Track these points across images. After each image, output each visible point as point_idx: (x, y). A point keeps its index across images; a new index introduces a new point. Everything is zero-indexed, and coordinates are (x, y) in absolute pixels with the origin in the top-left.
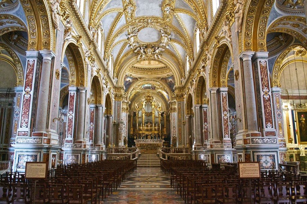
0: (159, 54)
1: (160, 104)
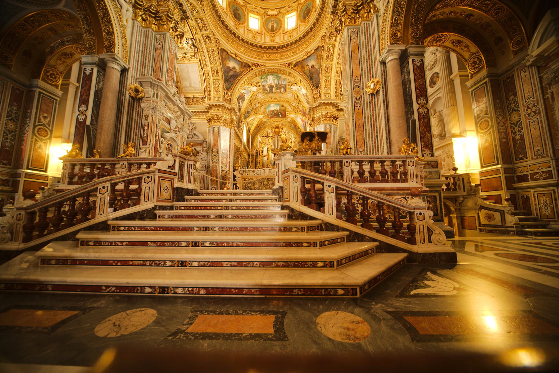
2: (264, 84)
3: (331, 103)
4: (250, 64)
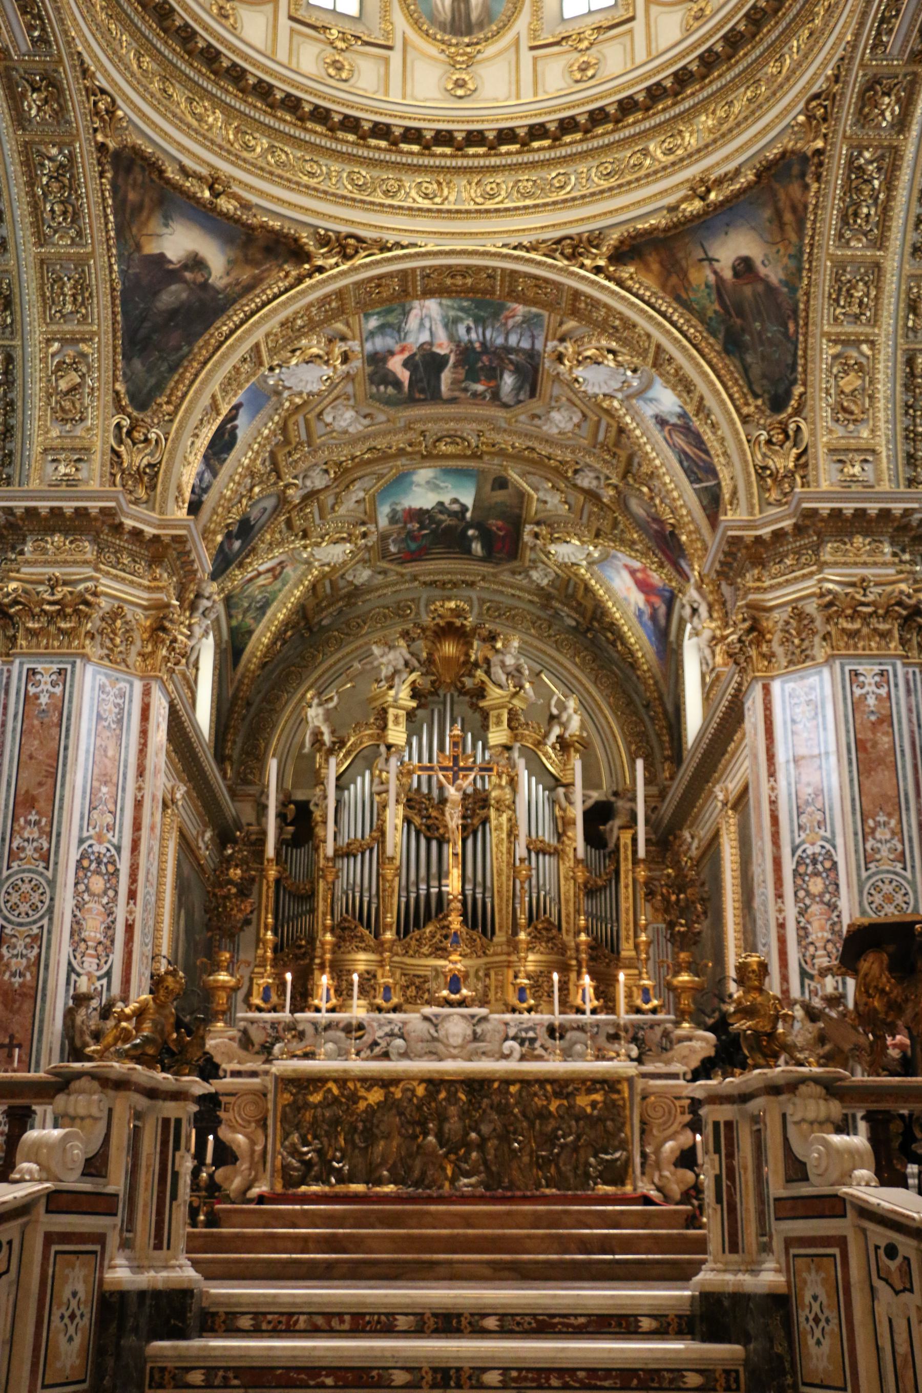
1: (572, 704)
2: (379, 343)
3: (885, 514)
4: (305, 238)
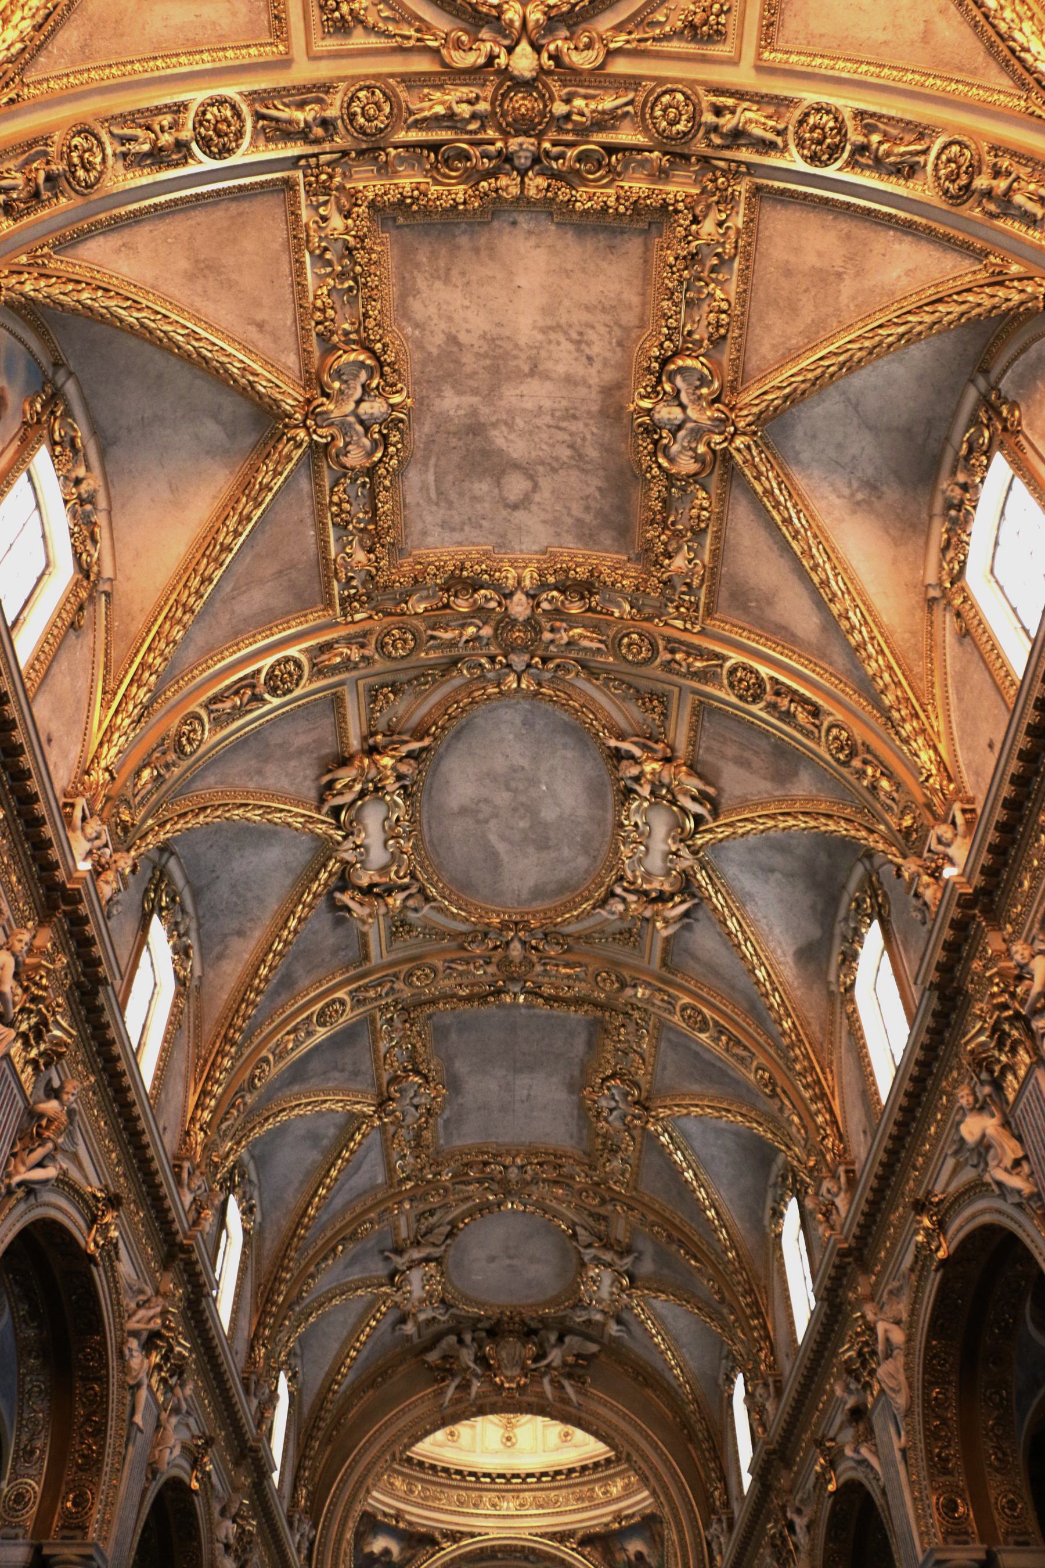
0: (570, 1376)
4: (437, 1535)
